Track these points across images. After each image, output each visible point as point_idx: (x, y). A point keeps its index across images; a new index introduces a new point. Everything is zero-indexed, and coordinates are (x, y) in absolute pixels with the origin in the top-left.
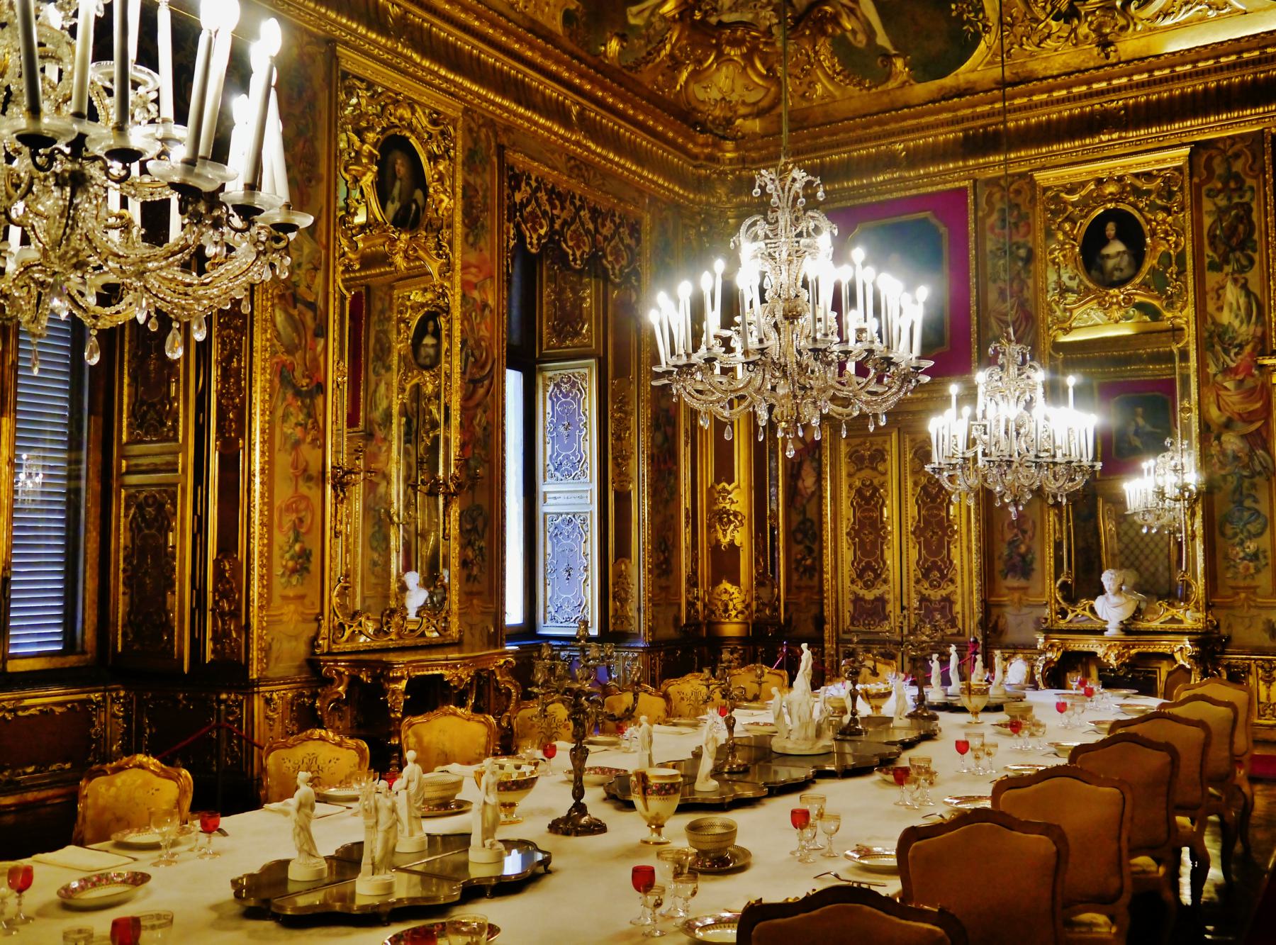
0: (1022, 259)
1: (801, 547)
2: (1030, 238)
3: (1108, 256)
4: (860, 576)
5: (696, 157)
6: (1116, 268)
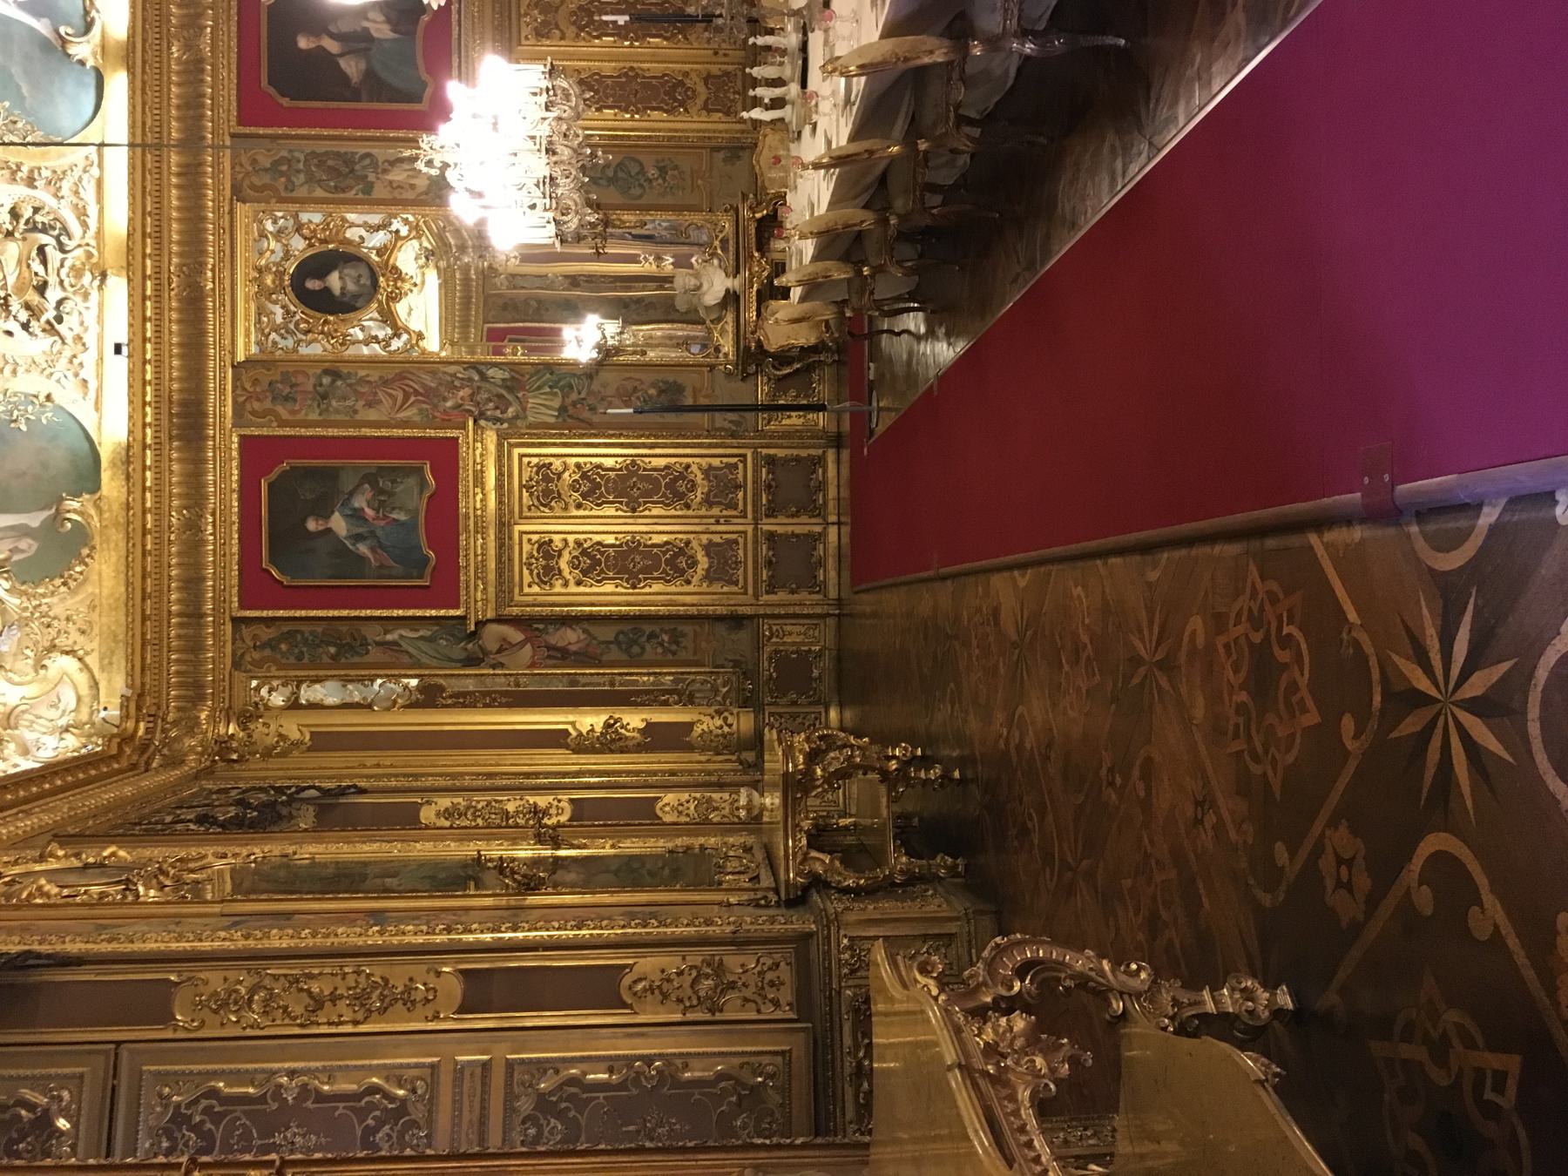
0: (334, 381)
1: (648, 647)
2: (311, 372)
3: (343, 288)
4: (682, 572)
5: (134, 767)
6: (357, 282)
